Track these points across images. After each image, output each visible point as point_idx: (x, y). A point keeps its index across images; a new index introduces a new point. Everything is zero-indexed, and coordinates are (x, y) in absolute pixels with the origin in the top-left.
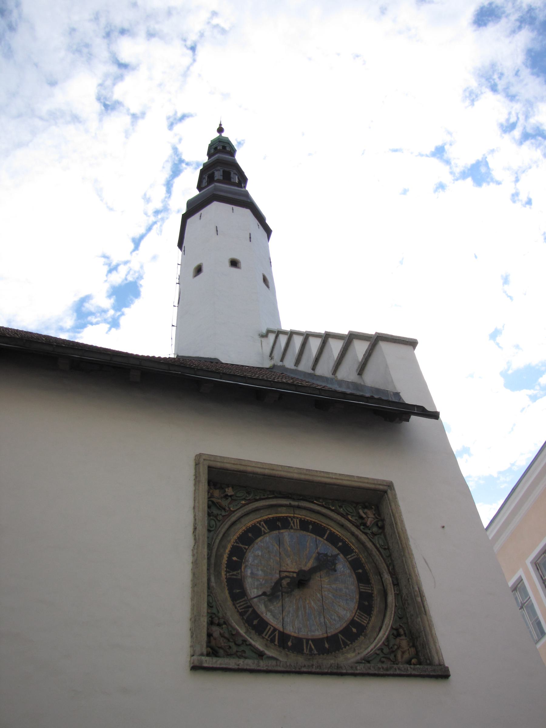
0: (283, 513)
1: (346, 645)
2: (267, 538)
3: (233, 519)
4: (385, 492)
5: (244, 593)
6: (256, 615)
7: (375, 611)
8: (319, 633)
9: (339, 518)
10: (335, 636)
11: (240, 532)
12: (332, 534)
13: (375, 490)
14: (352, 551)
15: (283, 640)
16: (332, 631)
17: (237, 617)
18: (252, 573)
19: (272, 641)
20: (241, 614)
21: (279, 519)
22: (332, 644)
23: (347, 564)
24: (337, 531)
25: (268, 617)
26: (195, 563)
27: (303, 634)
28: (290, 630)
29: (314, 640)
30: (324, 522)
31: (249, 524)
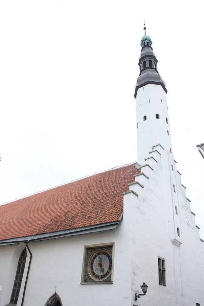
0: (100, 251)
2: (97, 257)
4: (112, 245)
13: (111, 245)
14: (110, 257)
15: (97, 277)
17: (91, 273)
20: (92, 273)
21: (99, 253)
23: (109, 260)
24: (108, 253)
25: (95, 273)
27: (100, 275)
28: (98, 274)
30: (106, 252)
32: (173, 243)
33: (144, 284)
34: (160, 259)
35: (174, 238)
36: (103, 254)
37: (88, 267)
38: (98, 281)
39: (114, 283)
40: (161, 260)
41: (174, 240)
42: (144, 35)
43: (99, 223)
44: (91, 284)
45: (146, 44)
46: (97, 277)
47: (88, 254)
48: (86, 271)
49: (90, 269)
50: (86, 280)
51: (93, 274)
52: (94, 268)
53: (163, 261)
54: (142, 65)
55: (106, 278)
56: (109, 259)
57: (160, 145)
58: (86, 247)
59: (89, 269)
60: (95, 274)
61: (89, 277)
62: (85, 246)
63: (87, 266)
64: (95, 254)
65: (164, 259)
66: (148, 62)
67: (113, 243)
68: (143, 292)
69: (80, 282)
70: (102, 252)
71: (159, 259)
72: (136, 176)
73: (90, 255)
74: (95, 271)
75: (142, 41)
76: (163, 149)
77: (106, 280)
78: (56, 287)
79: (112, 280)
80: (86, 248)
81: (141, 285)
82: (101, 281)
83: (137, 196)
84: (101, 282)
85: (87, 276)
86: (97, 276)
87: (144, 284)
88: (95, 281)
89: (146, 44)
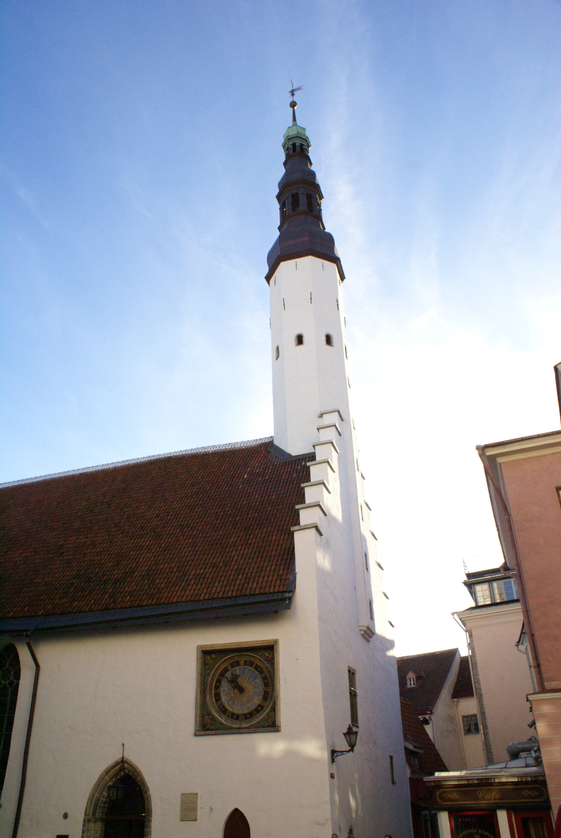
1: (255, 715)
3: (216, 667)
5: (220, 699)
6: (224, 707)
7: (269, 700)
8: (246, 711)
9: (258, 657)
10: (252, 712)
11: (220, 671)
12: (257, 665)
16: (250, 710)
18: (224, 690)
19: (229, 716)
20: (219, 707)
22: (249, 716)
24: (259, 663)
26: (197, 693)
28: (235, 711)
29: (243, 714)
30: (253, 659)
31: (224, 667)
32: (362, 635)
35: (367, 625)
36: (245, 664)
38: (237, 726)
39: (283, 728)
41: (365, 629)
42: (290, 123)
45: (298, 149)
46: (232, 717)
47: (207, 664)
48: (204, 703)
50: (207, 725)
51: (223, 710)
52: (224, 698)
53: (353, 674)
54: (289, 202)
55: (264, 717)
56: (263, 675)
57: (339, 411)
58: (204, 649)
60: (226, 710)
63: (204, 693)
65: (354, 671)
66: (300, 197)
67: (276, 642)
68: (350, 746)
70: (243, 661)
71: (349, 671)
72: (307, 486)
74: (226, 704)
75: (289, 139)
76: (342, 420)
77: (258, 722)
81: (345, 731)
82: (243, 726)
83: (321, 534)
84: (246, 728)
85: (208, 715)
86: (233, 714)
88: (230, 728)
89: (298, 149)
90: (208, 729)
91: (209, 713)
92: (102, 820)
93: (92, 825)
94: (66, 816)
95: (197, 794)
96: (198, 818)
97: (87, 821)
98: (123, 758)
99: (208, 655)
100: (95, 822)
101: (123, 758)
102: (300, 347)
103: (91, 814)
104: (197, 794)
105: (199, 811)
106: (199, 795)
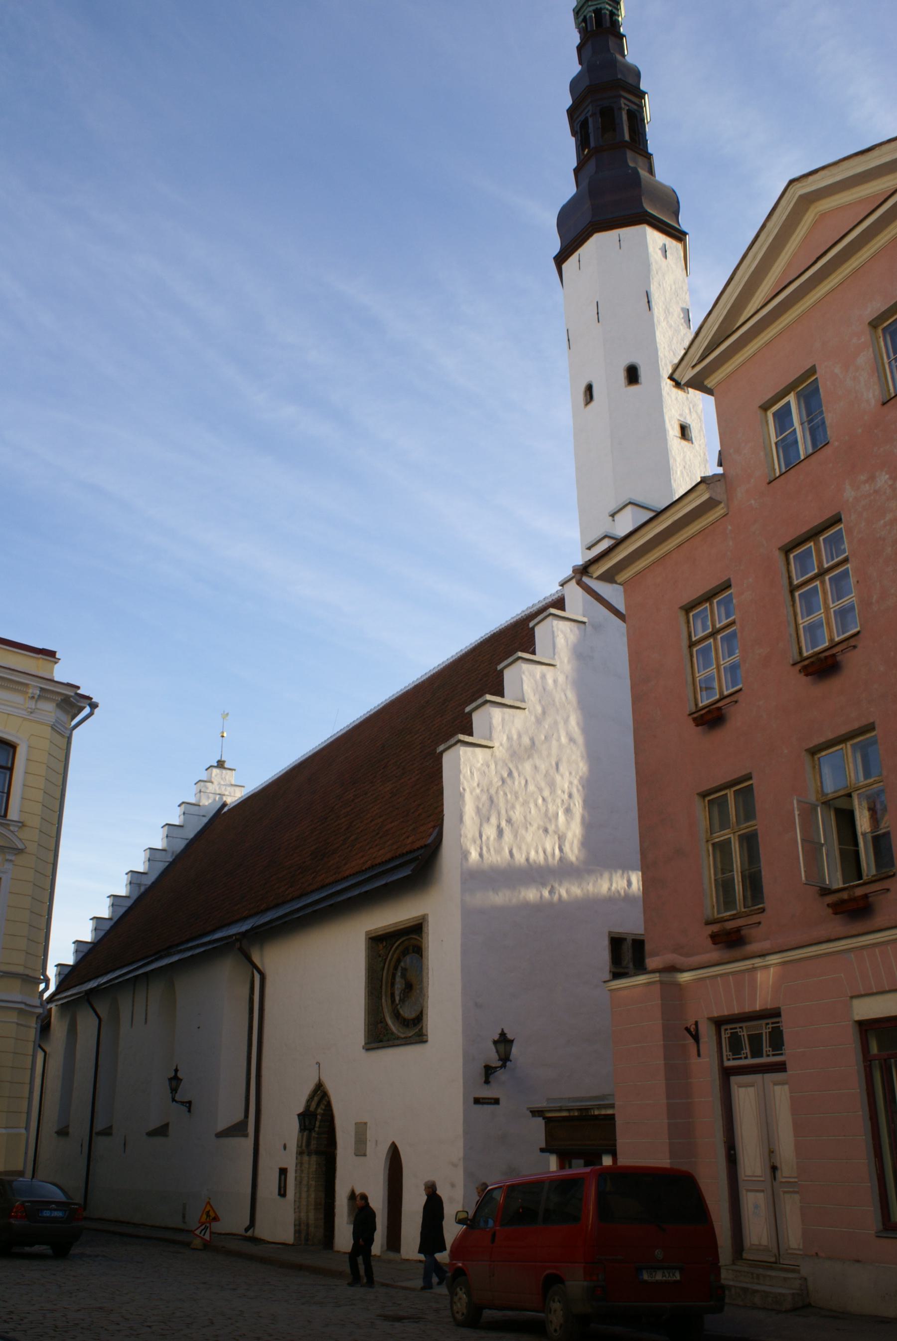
25: (401, 1012)
33: (503, 1034)
34: (625, 939)
37: (384, 997)
39: (429, 1039)
40: (629, 942)
43: (389, 856)
44: (383, 1047)
49: (389, 1001)
50: (378, 1036)
59: (385, 1002)
60: (399, 1014)
61: (387, 1025)
62: (367, 933)
64: (398, 951)
69: (363, 1043)
73: (386, 959)
78: (318, 1064)
79: (424, 1031)
80: (370, 938)
87: (503, 1034)
88: (398, 1038)
90: (381, 1041)
91: (383, 1021)
92: (317, 1153)
93: (306, 1158)
94: (285, 1147)
95: (366, 1124)
96: (368, 1153)
97: (300, 1153)
98: (320, 1080)
99: (379, 942)
100: (309, 1154)
101: (320, 1080)
102: (634, 388)
103: (304, 1144)
104: (366, 1124)
105: (368, 1144)
106: (368, 1125)
